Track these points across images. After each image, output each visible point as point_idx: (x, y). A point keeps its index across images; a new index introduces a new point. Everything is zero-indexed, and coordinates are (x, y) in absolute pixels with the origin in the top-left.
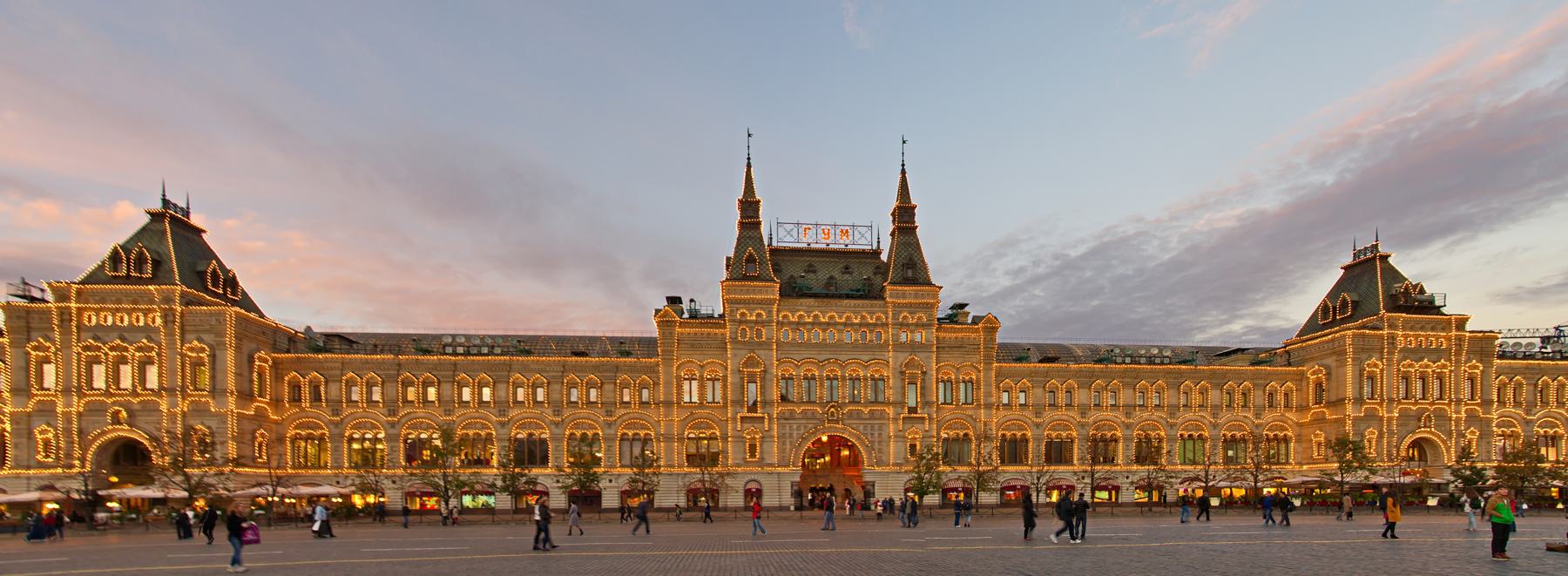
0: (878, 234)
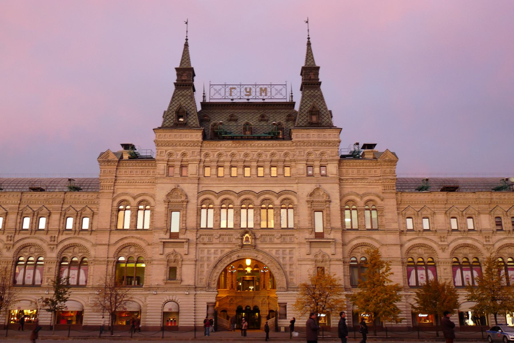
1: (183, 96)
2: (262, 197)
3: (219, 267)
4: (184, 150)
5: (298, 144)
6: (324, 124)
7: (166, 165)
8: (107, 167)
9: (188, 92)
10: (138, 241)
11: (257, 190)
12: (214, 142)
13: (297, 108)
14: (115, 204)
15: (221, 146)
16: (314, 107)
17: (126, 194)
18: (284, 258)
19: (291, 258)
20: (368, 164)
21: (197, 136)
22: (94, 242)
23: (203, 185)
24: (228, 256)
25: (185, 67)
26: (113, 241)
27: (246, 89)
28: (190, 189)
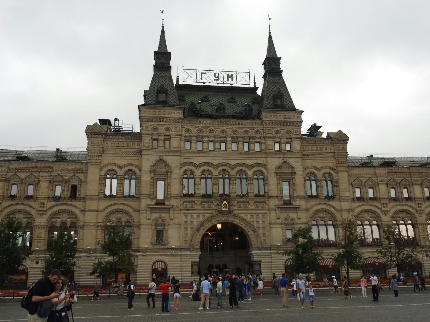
0: (252, 76)
1: (162, 77)
2: (237, 169)
3: (201, 230)
4: (167, 126)
5: (267, 123)
6: (287, 107)
7: (150, 138)
8: (95, 139)
9: (166, 74)
10: (126, 208)
11: (233, 162)
12: (193, 120)
13: (259, 92)
14: (103, 173)
15: (200, 123)
16: (279, 92)
17: (113, 164)
18: (257, 222)
19: (264, 222)
20: (324, 142)
21: (178, 114)
22: (83, 209)
23: (184, 157)
24: (209, 220)
25: (163, 51)
26: (101, 208)
27: (215, 74)
28: (173, 160)
